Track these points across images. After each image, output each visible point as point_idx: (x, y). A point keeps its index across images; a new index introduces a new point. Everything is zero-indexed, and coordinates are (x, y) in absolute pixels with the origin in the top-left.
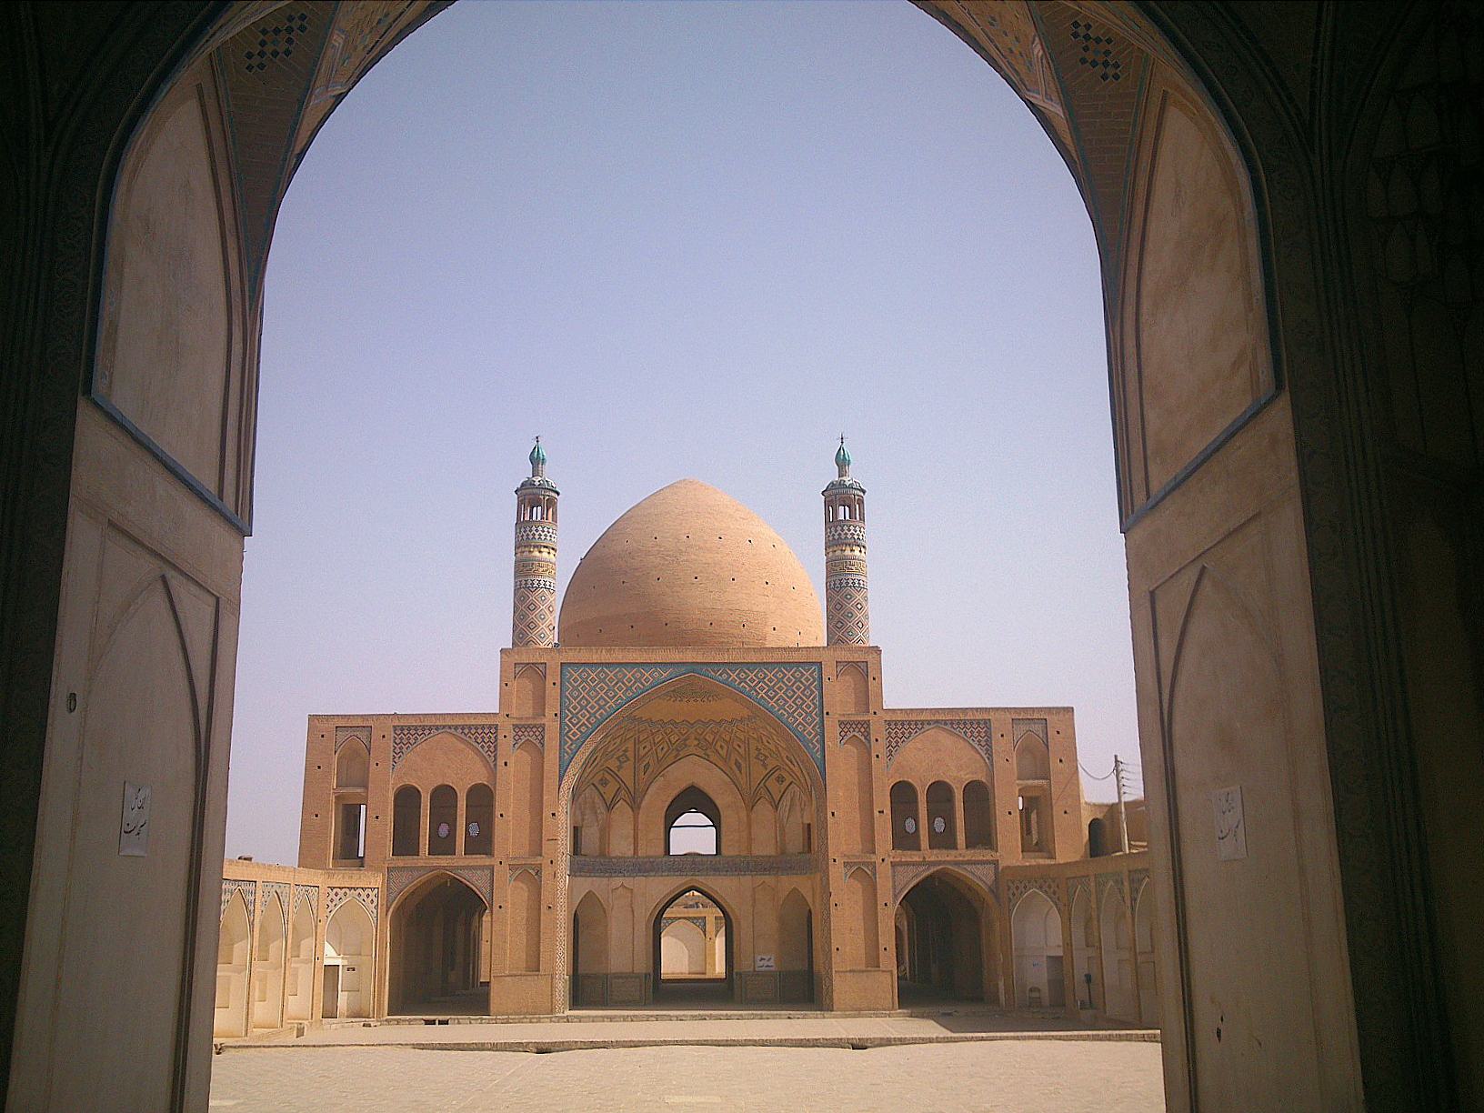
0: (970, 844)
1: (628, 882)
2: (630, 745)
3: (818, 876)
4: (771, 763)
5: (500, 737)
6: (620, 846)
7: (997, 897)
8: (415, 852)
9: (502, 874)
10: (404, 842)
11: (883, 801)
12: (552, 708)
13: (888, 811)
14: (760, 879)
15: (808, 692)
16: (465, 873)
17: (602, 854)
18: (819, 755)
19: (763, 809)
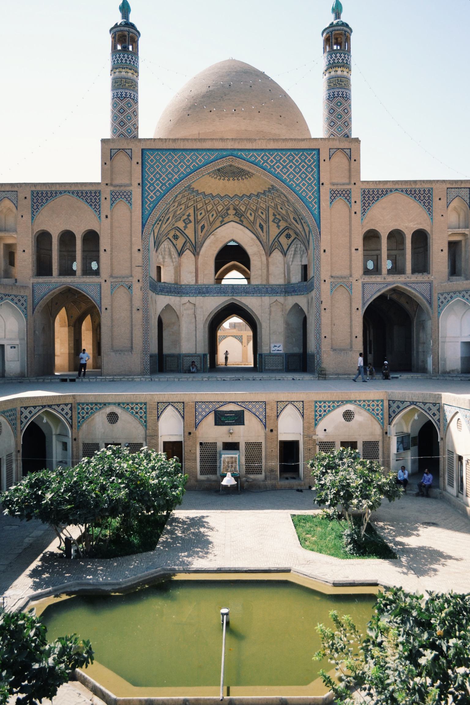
0: (414, 271)
1: (192, 299)
2: (191, 211)
3: (313, 293)
4: (283, 225)
5: (103, 199)
6: (187, 279)
7: (430, 304)
8: (49, 273)
9: (106, 288)
10: (43, 268)
11: (358, 242)
12: (137, 178)
13: (361, 249)
14: (275, 298)
15: (309, 170)
16: (82, 287)
17: (176, 284)
18: (316, 212)
19: (277, 255)
